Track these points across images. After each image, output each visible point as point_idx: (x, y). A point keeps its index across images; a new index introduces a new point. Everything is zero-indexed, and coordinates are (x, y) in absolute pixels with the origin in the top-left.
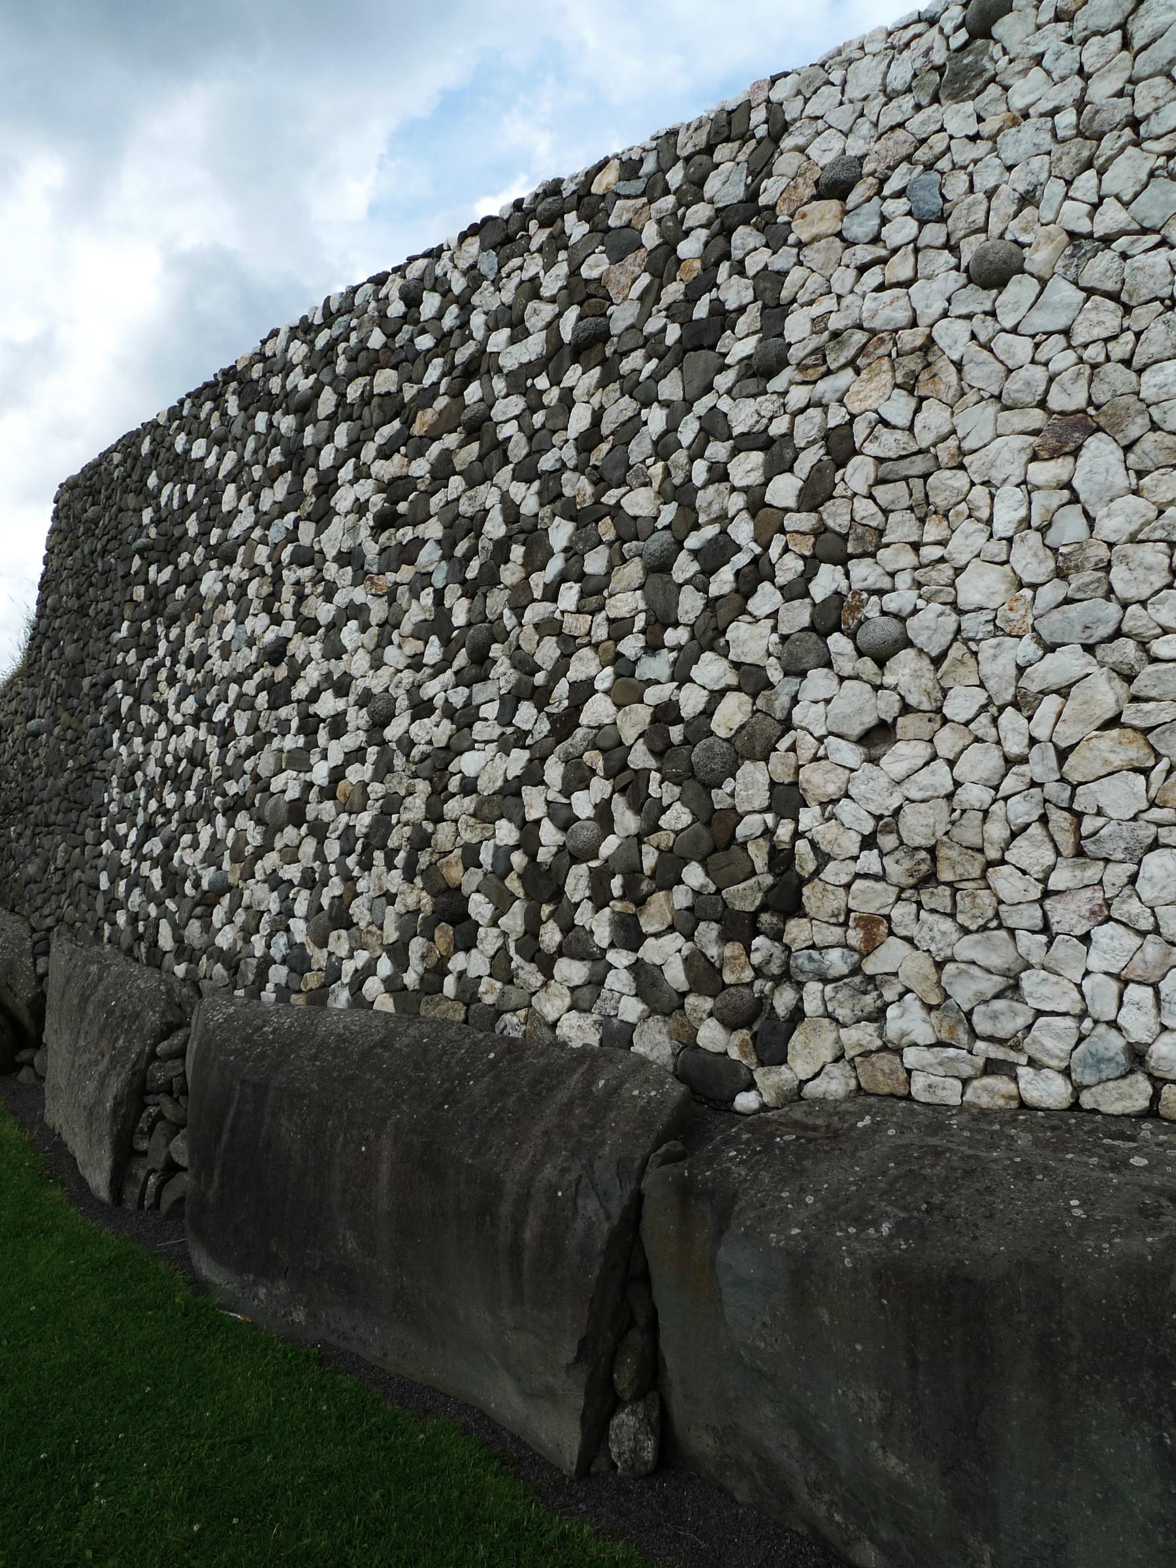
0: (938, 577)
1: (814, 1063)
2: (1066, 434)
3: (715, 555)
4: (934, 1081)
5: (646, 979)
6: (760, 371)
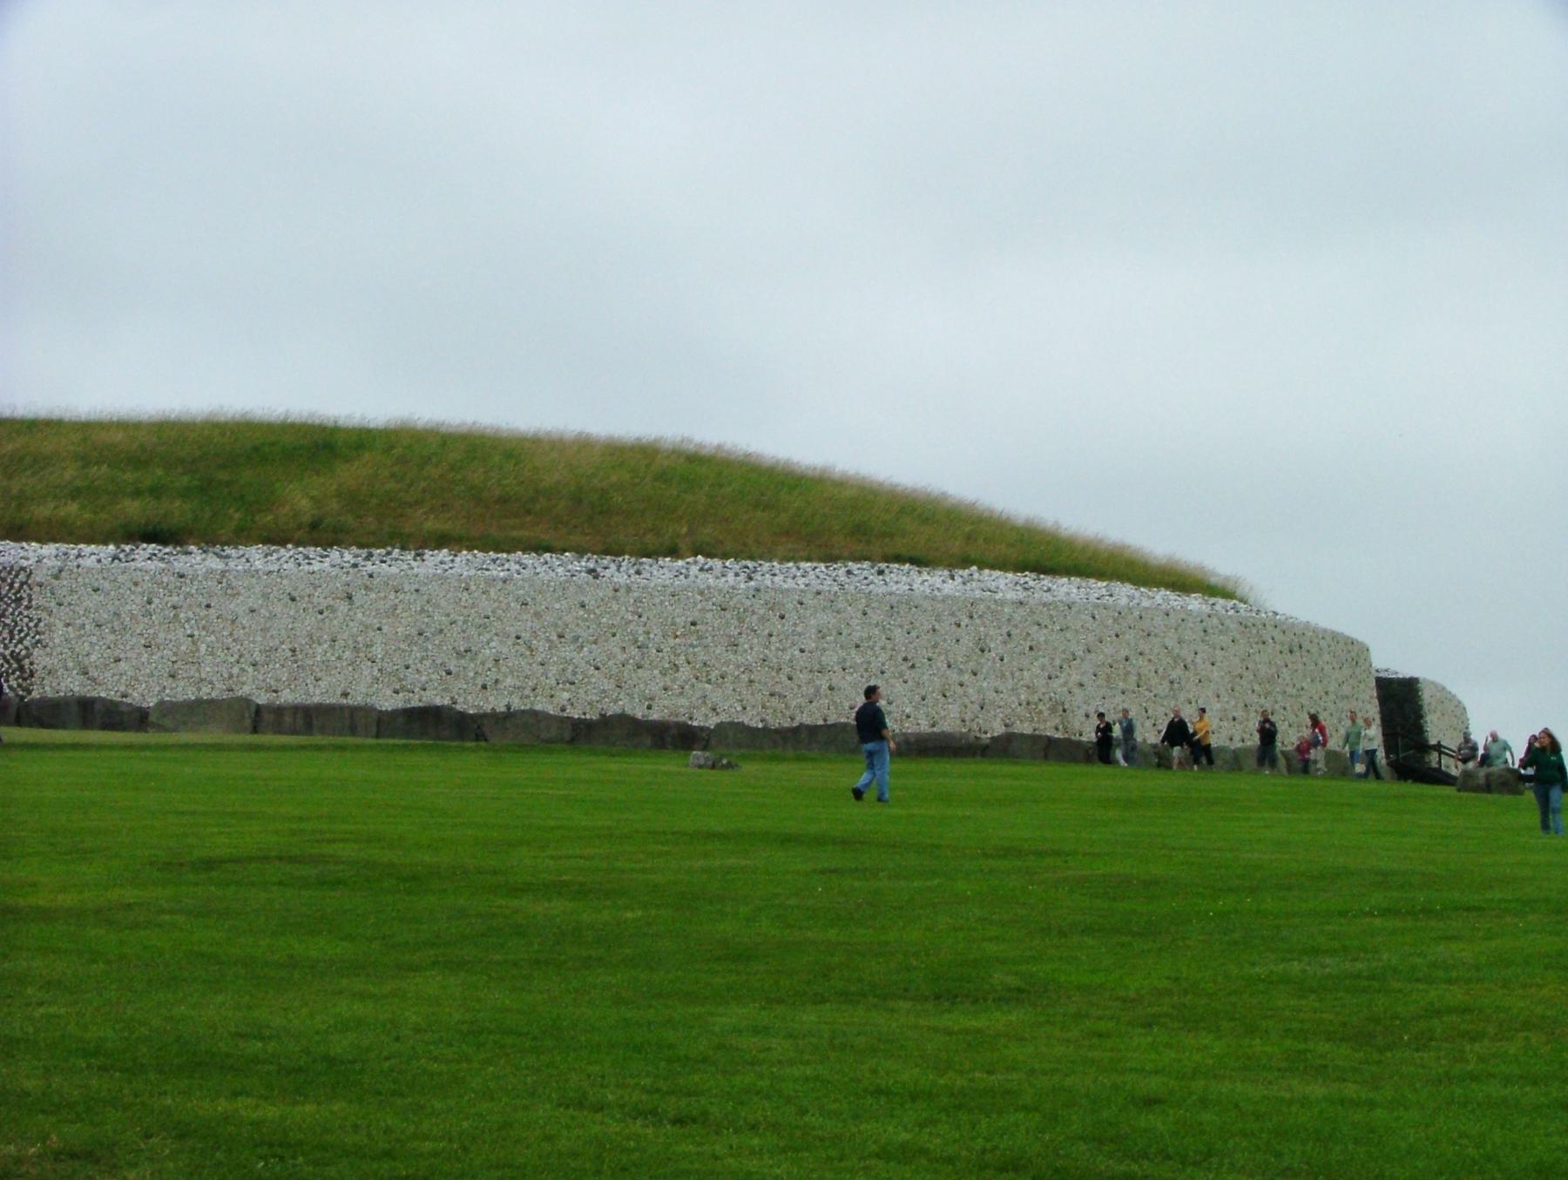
0: (52, 639)
1: (35, 695)
2: (68, 625)
3: (21, 631)
4: (50, 695)
5: (10, 687)
6: (28, 608)
